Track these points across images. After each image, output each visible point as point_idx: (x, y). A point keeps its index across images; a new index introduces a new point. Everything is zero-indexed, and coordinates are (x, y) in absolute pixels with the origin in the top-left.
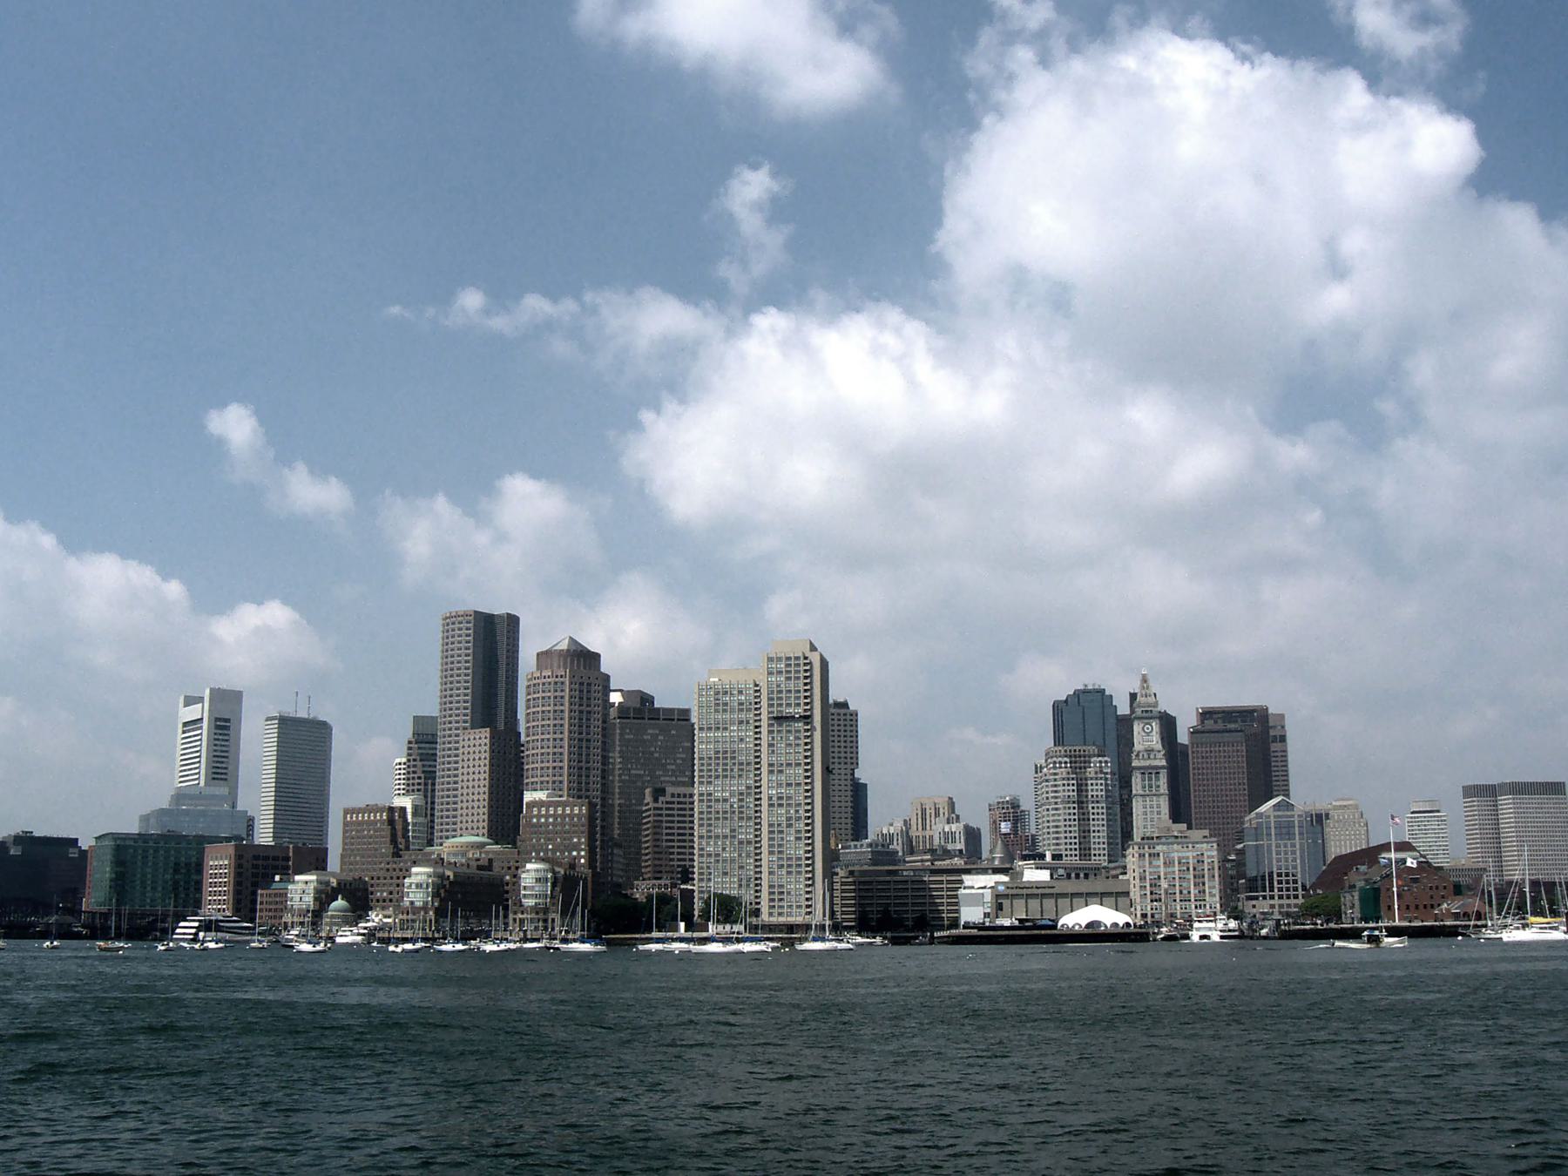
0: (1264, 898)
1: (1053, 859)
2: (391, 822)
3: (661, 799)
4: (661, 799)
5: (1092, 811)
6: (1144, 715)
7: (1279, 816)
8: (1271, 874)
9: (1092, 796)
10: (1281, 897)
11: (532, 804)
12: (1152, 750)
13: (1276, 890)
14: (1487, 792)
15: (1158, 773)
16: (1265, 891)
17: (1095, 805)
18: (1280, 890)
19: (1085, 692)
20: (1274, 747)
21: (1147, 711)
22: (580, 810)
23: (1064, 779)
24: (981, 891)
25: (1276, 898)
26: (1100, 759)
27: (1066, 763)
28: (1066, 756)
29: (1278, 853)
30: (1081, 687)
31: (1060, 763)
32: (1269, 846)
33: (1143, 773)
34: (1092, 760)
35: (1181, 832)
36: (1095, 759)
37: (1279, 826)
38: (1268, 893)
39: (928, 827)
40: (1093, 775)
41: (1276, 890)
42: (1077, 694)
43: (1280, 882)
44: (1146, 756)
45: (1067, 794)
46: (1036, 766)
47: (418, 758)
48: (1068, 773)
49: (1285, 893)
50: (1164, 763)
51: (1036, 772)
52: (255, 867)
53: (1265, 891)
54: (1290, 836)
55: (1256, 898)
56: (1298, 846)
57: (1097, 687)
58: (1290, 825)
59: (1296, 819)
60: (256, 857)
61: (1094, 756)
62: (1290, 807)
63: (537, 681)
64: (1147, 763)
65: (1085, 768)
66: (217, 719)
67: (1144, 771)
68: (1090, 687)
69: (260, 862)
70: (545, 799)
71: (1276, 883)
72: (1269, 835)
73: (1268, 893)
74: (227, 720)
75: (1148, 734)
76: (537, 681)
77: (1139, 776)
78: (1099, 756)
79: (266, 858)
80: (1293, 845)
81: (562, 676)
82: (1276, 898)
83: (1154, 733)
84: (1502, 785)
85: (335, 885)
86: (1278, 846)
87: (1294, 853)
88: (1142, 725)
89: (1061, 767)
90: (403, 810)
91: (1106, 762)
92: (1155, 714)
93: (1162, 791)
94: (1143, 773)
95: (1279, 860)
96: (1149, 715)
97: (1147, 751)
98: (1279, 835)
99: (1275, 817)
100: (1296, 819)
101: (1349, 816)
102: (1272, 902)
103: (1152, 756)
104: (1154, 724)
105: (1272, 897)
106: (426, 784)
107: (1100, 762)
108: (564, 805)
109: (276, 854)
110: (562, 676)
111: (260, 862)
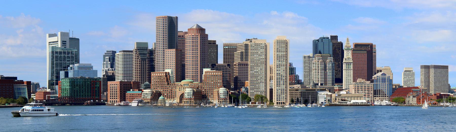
0: (378, 97)
1: (321, 85)
2: (166, 76)
3: (215, 67)
4: (215, 67)
5: (328, 72)
6: (348, 49)
7: (382, 77)
8: (380, 90)
9: (328, 68)
10: (382, 97)
11: (206, 72)
12: (349, 58)
13: (381, 95)
14: (427, 68)
15: (350, 64)
16: (378, 95)
17: (329, 70)
18: (382, 95)
19: (324, 38)
20: (374, 54)
21: (348, 48)
22: (220, 74)
23: (321, 63)
24: (323, 95)
25: (381, 97)
26: (330, 58)
27: (321, 58)
28: (321, 57)
29: (382, 86)
30: (323, 37)
31: (320, 59)
32: (380, 84)
33: (347, 64)
34: (328, 58)
35: (364, 81)
36: (329, 58)
37: (382, 79)
38: (379, 95)
39: (272, 73)
40: (328, 62)
41: (381, 95)
43: (382, 93)
44: (347, 60)
46: (304, 56)
47: (139, 54)
48: (322, 61)
49: (383, 96)
51: (304, 58)
52: (124, 87)
53: (378, 95)
54: (385, 82)
55: (376, 97)
56: (387, 84)
58: (385, 79)
59: (387, 78)
60: (124, 85)
61: (329, 57)
62: (385, 74)
63: (190, 37)
64: (348, 61)
65: (326, 60)
66: (63, 41)
67: (347, 63)
68: (325, 37)
69: (125, 86)
70: (210, 71)
72: (380, 81)
73: (379, 95)
74: (66, 42)
76: (190, 37)
77: (346, 65)
78: (330, 57)
79: (126, 85)
80: (385, 84)
81: (197, 36)
85: (155, 92)
86: (382, 84)
87: (385, 86)
89: (320, 60)
90: (169, 73)
91: (332, 59)
92: (350, 49)
93: (351, 69)
94: (347, 64)
95: (382, 88)
96: (349, 49)
97: (348, 58)
98: (382, 82)
99: (381, 77)
100: (387, 78)
101: (388, 72)
102: (380, 98)
103: (349, 60)
104: (350, 51)
105: (380, 97)
106: (142, 62)
107: (330, 59)
108: (214, 72)
109: (126, 84)
110: (197, 36)
111: (125, 86)
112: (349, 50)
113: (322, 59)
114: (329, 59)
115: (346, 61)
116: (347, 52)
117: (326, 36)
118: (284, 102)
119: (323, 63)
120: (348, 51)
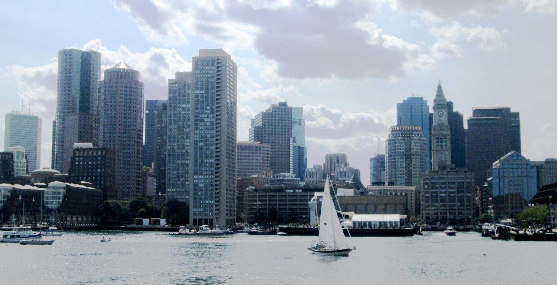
13: (509, 204)
18: (512, 203)
21: (440, 104)
26: (418, 132)
27: (399, 134)
36: (415, 132)
41: (509, 204)
45: (399, 151)
50: (449, 132)
64: (440, 132)
68: (416, 96)
71: (509, 200)
75: (441, 117)
83: (444, 117)
88: (437, 112)
104: (444, 111)
112: (442, 110)
113: (401, 136)
115: (437, 133)
116: (438, 114)
118: (212, 220)
120: (440, 111)
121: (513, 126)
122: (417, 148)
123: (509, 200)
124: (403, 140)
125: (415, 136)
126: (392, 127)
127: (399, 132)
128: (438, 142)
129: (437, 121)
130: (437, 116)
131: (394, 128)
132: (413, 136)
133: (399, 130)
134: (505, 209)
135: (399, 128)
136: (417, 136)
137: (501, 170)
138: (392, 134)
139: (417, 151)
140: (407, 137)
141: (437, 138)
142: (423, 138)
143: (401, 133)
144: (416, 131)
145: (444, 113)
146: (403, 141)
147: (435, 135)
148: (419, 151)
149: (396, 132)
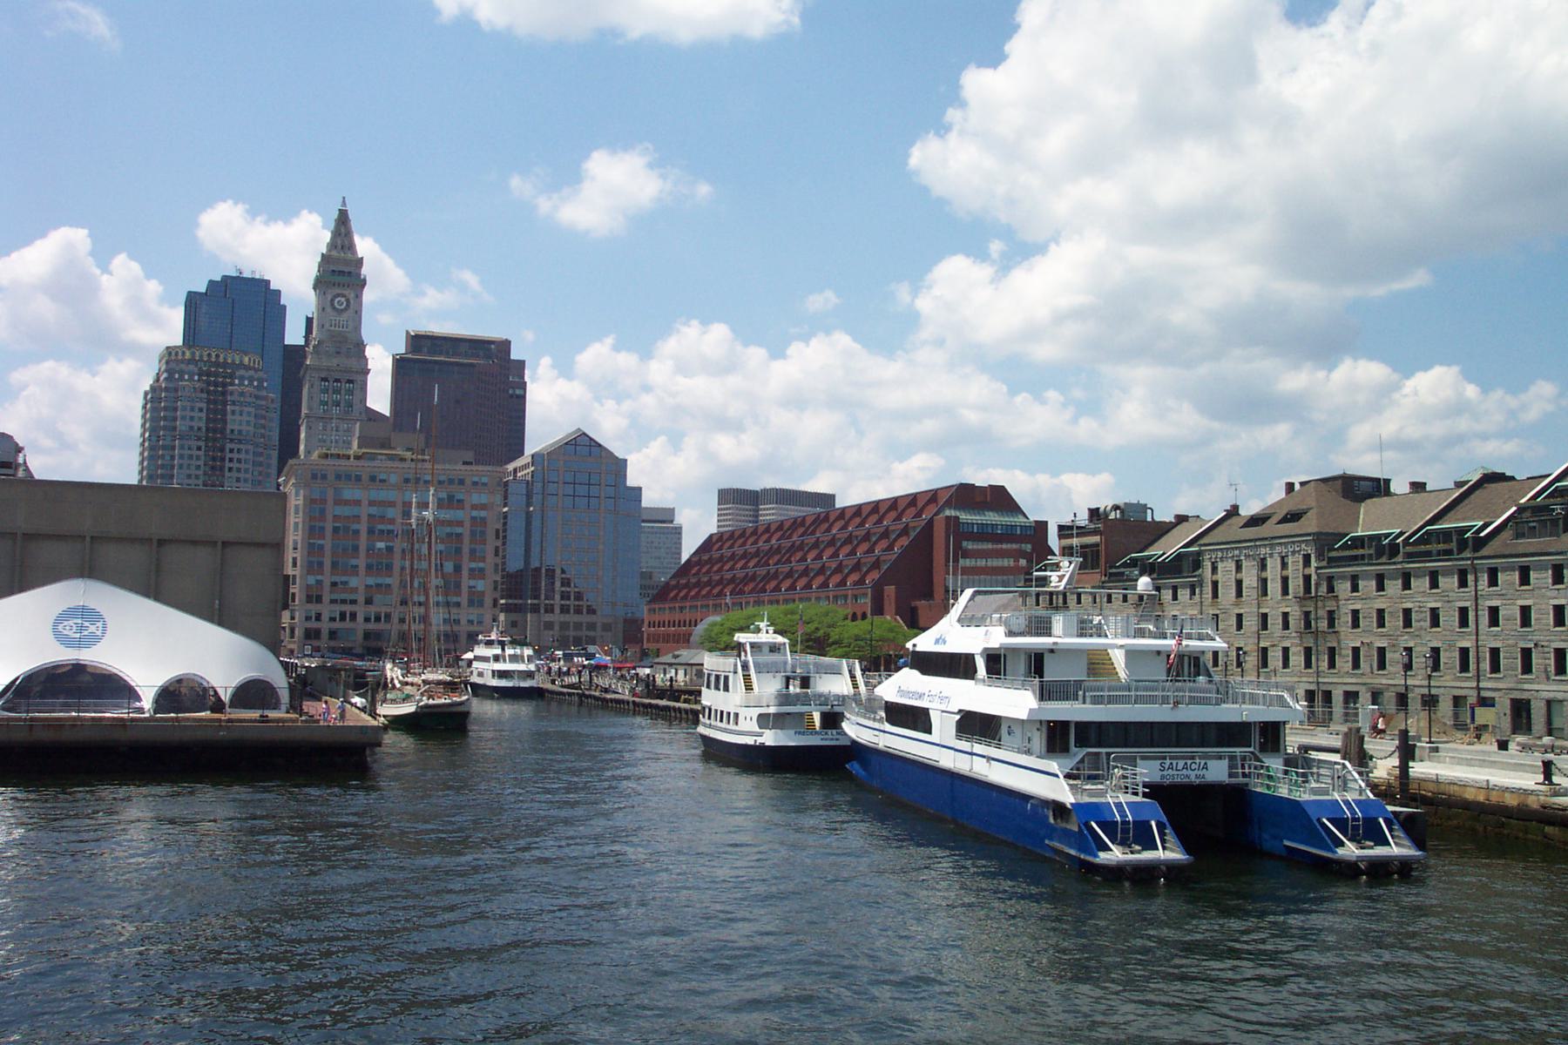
0: (535, 609)
10: (565, 610)
13: (557, 597)
16: (537, 597)
18: (565, 596)
21: (341, 273)
25: (557, 610)
26: (251, 373)
30: (234, 274)
36: (242, 372)
42: (225, 278)
49: (572, 602)
57: (258, 277)
64: (335, 362)
65: (224, 385)
68: (247, 275)
71: (558, 584)
82: (557, 610)
84: (765, 491)
102: (548, 617)
105: (549, 609)
113: (196, 378)
114: (242, 378)
116: (332, 304)
117: (253, 272)
119: (201, 400)
120: (338, 295)
121: (511, 396)
122: (245, 418)
123: (558, 584)
124: (202, 391)
125: (241, 384)
126: (168, 348)
127: (191, 367)
128: (326, 391)
129: (327, 326)
130: (329, 309)
131: (177, 354)
132: (237, 381)
133: (192, 361)
134: (542, 611)
135: (193, 354)
136: (246, 383)
137: (538, 486)
138: (166, 371)
139: (244, 428)
140: (216, 384)
141: (325, 379)
142: (264, 393)
143: (196, 370)
144: (247, 368)
145: (352, 302)
146: (205, 395)
147: (318, 369)
148: (251, 428)
149: (183, 366)
